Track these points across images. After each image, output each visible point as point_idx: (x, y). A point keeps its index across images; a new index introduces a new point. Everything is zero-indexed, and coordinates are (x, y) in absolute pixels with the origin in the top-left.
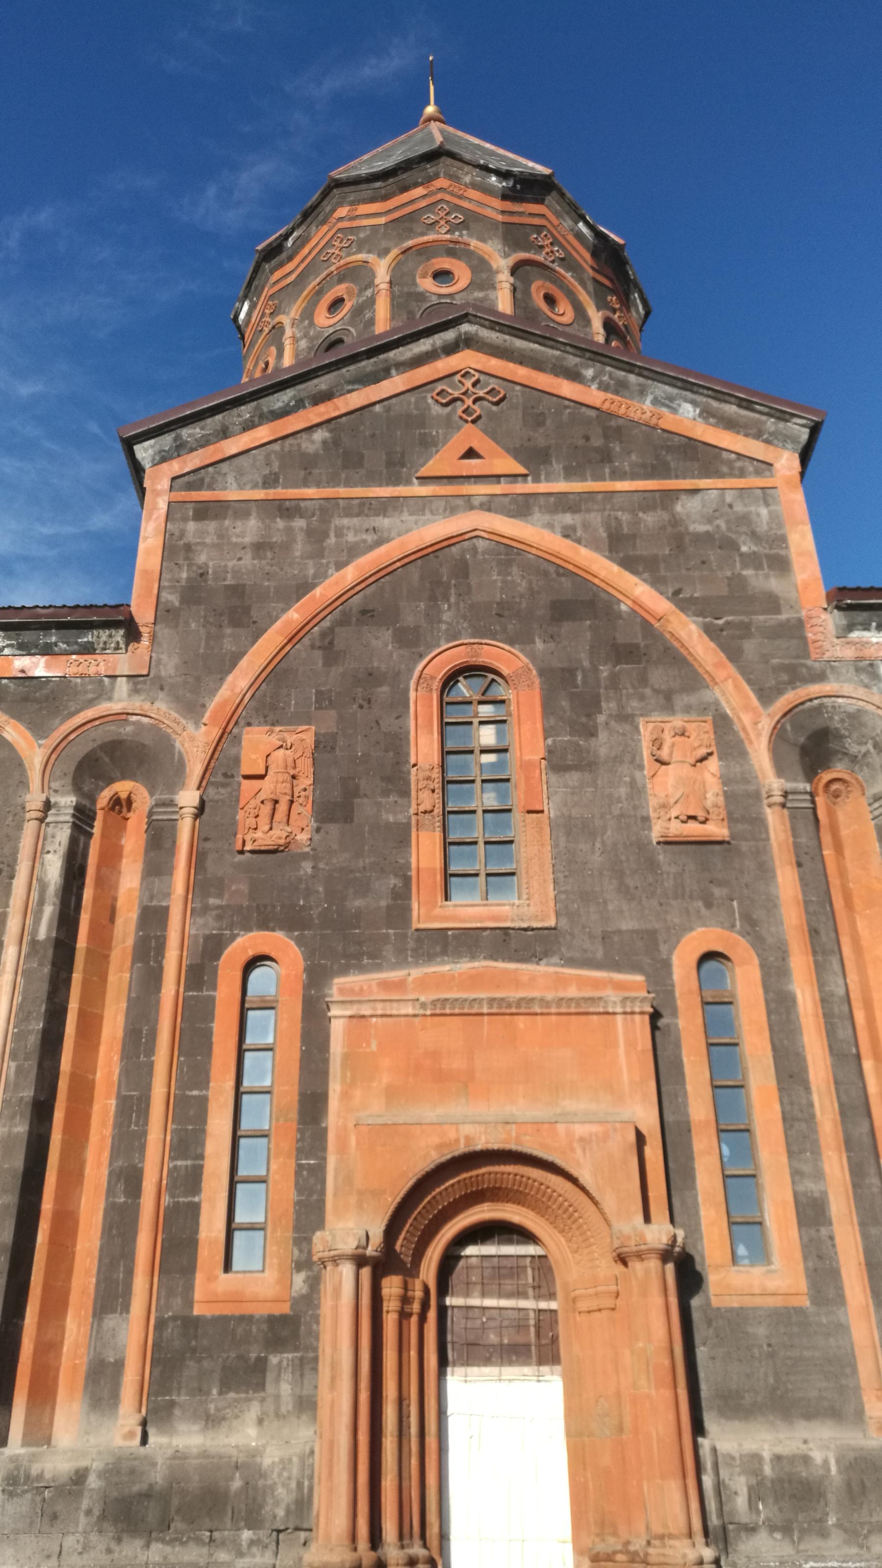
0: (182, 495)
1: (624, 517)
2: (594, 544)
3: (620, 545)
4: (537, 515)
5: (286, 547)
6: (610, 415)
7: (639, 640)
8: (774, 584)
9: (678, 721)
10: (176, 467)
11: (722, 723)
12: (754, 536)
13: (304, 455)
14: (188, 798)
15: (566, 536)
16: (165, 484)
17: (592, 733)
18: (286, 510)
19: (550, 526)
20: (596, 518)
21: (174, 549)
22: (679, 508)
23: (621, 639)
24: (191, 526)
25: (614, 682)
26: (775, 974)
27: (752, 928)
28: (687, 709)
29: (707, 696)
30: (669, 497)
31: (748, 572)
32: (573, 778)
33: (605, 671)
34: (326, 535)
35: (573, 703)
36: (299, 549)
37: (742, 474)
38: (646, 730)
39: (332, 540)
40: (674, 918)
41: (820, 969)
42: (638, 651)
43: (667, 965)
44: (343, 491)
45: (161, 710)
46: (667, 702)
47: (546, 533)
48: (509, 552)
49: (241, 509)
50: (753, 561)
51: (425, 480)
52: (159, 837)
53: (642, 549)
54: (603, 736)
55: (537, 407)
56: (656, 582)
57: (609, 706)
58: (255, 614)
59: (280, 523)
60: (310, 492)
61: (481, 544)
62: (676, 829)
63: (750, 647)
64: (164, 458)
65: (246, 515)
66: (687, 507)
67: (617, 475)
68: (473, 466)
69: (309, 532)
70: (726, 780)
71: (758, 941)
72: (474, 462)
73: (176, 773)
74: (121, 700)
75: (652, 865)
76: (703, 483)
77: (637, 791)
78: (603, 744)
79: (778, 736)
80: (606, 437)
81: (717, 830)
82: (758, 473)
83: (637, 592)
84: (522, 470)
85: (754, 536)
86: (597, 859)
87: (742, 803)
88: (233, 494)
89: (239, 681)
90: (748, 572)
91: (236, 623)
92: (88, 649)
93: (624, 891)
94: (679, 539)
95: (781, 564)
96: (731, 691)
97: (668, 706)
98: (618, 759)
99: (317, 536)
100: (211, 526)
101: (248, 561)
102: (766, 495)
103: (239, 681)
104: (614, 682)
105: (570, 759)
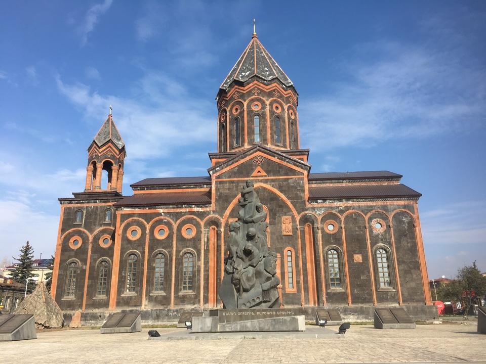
0: (217, 180)
1: (281, 183)
2: (276, 188)
3: (281, 189)
4: (269, 183)
5: (233, 188)
6: (280, 164)
7: (282, 204)
8: (302, 195)
9: (287, 217)
10: (215, 175)
11: (293, 217)
12: (300, 186)
13: (234, 172)
14: (222, 230)
15: (273, 187)
16: (214, 178)
17: (275, 219)
18: (232, 182)
19: (270, 185)
20: (277, 183)
21: (217, 189)
22: (289, 181)
23: (280, 204)
24: (219, 185)
25: (279, 210)
26: (296, 253)
27: (294, 247)
28: (288, 215)
29: (291, 213)
30: (288, 179)
31: (298, 193)
32: (272, 226)
33: (277, 209)
34: (238, 187)
35: (273, 214)
36: (234, 189)
37: (299, 175)
38: (282, 218)
39: (239, 187)
40: (284, 246)
41: (302, 252)
42: (282, 206)
43: (283, 252)
44: (240, 179)
45: (217, 216)
46: (285, 214)
47: (270, 186)
48: (264, 189)
49: (226, 182)
50: (299, 190)
51: (252, 177)
52: (218, 235)
53: (284, 189)
54: (277, 219)
55: (269, 163)
56: (285, 194)
57: (278, 215)
58: (229, 200)
59: (232, 184)
60: (235, 179)
61: (261, 188)
62: (285, 233)
63: (297, 205)
64: (214, 173)
65: (226, 183)
66: (290, 181)
67: (281, 175)
68: (259, 174)
69: (236, 186)
70: (292, 226)
71: (294, 249)
72: (259, 173)
73: (221, 227)
74: (212, 215)
75: (282, 238)
76: (293, 177)
77: (281, 228)
78: (276, 221)
79: (300, 220)
80: (279, 168)
81: (291, 234)
82: (301, 175)
83: (282, 196)
84: (266, 175)
85: (300, 186)
86: (275, 238)
87: (295, 229)
88: (225, 180)
89: (228, 212)
90: (298, 193)
91: (226, 202)
92: (207, 207)
93: (278, 242)
94: (289, 187)
95: (303, 191)
96: (295, 212)
97: (286, 215)
98: (279, 223)
99: (237, 187)
100: (222, 185)
101: (227, 190)
102: (302, 179)
103: (228, 212)
104: (278, 211)
105: (272, 223)
